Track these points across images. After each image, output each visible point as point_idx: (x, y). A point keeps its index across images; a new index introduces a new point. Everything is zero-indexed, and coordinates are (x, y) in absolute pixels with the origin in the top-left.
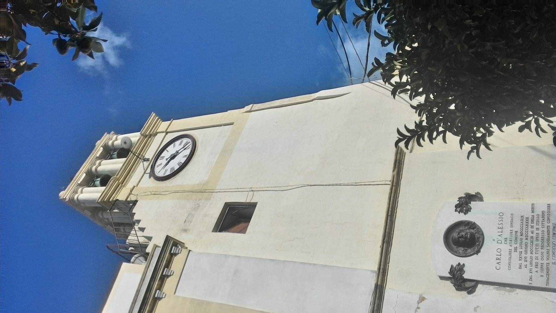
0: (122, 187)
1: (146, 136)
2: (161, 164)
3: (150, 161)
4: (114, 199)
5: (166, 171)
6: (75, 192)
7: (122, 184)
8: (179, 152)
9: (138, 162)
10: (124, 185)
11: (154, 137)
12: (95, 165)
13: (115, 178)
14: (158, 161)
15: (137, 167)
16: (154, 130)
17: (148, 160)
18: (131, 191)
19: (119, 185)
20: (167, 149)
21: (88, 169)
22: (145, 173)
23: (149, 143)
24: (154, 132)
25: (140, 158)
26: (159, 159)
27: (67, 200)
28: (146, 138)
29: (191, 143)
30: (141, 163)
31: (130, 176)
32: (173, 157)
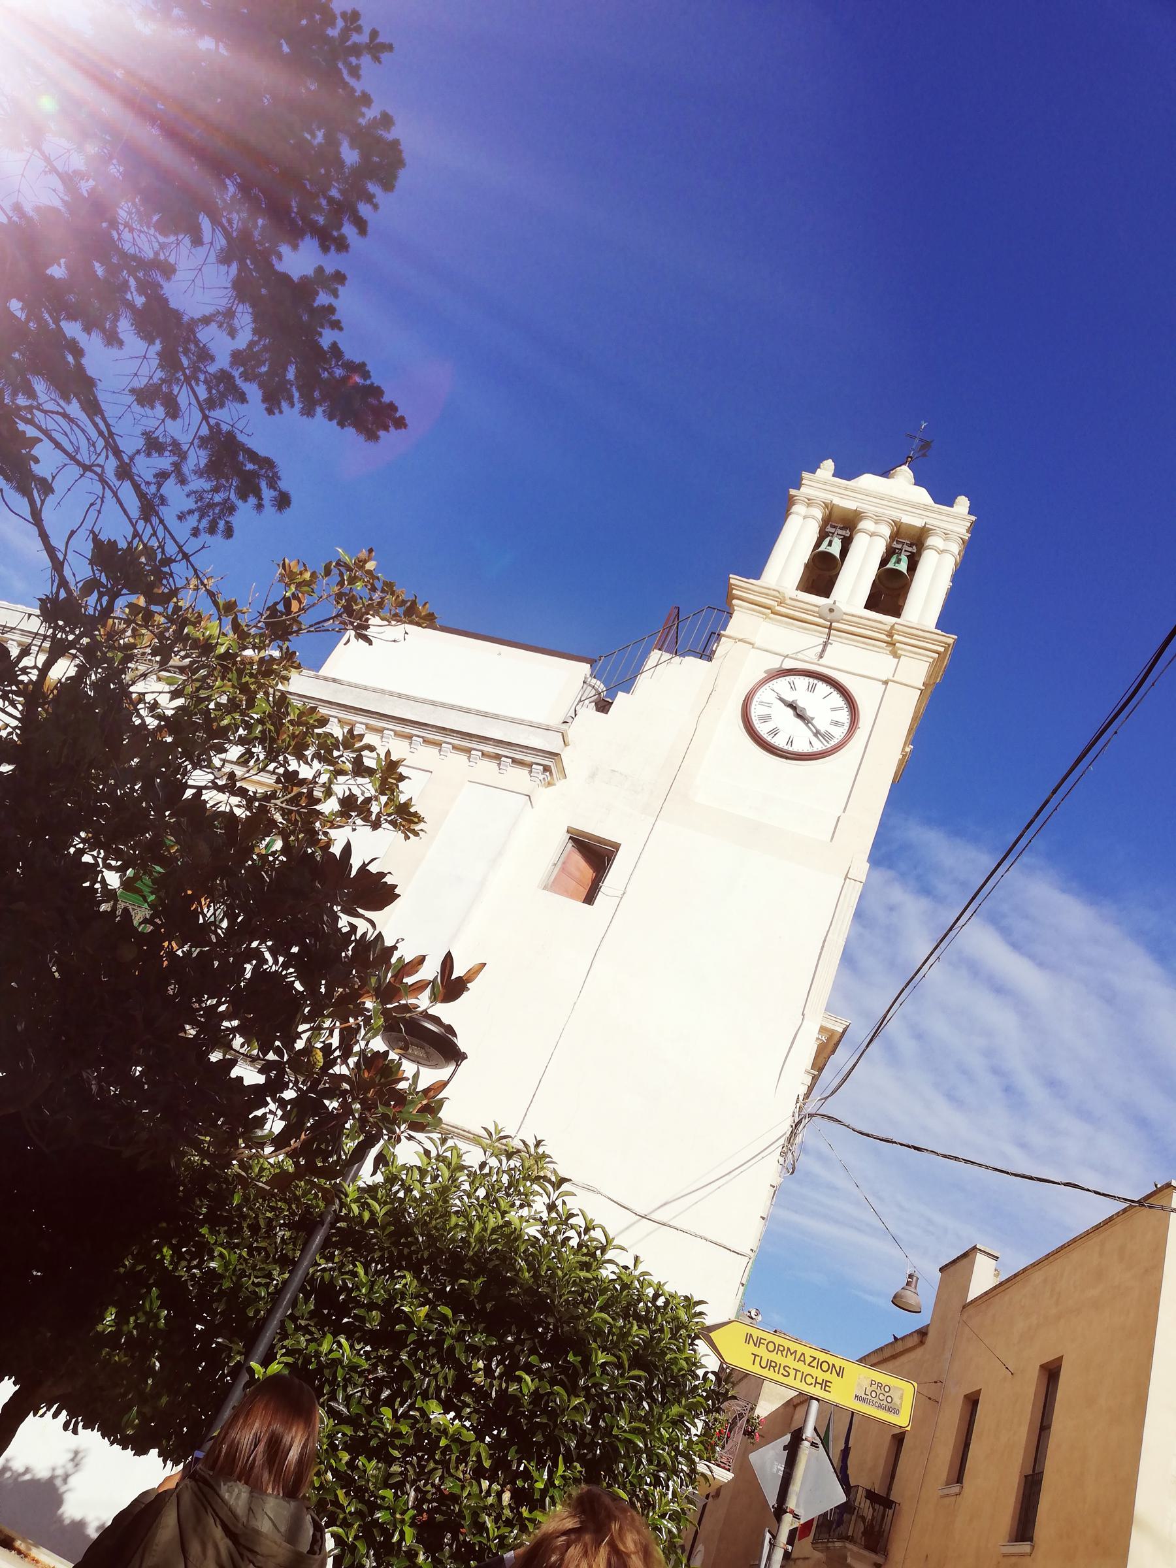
0: (764, 616)
1: (890, 635)
2: (793, 687)
3: (816, 661)
4: (736, 608)
5: (769, 705)
6: (810, 502)
7: (772, 613)
8: (810, 725)
9: (821, 633)
10: (770, 618)
11: (888, 652)
12: (876, 523)
13: (784, 597)
14: (807, 678)
15: (814, 633)
16: (905, 650)
17: (821, 657)
18: (740, 640)
19: (769, 608)
20: (836, 692)
21: (864, 513)
22: (787, 656)
23: (873, 646)
24: (899, 652)
25: (829, 634)
26: (811, 680)
27: (792, 492)
28: (887, 635)
29: (829, 746)
30: (821, 641)
31: (792, 624)
32: (800, 715)
